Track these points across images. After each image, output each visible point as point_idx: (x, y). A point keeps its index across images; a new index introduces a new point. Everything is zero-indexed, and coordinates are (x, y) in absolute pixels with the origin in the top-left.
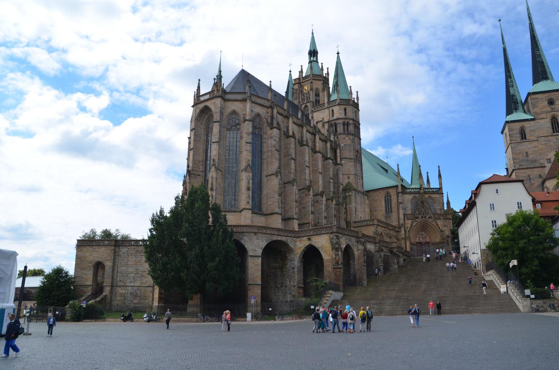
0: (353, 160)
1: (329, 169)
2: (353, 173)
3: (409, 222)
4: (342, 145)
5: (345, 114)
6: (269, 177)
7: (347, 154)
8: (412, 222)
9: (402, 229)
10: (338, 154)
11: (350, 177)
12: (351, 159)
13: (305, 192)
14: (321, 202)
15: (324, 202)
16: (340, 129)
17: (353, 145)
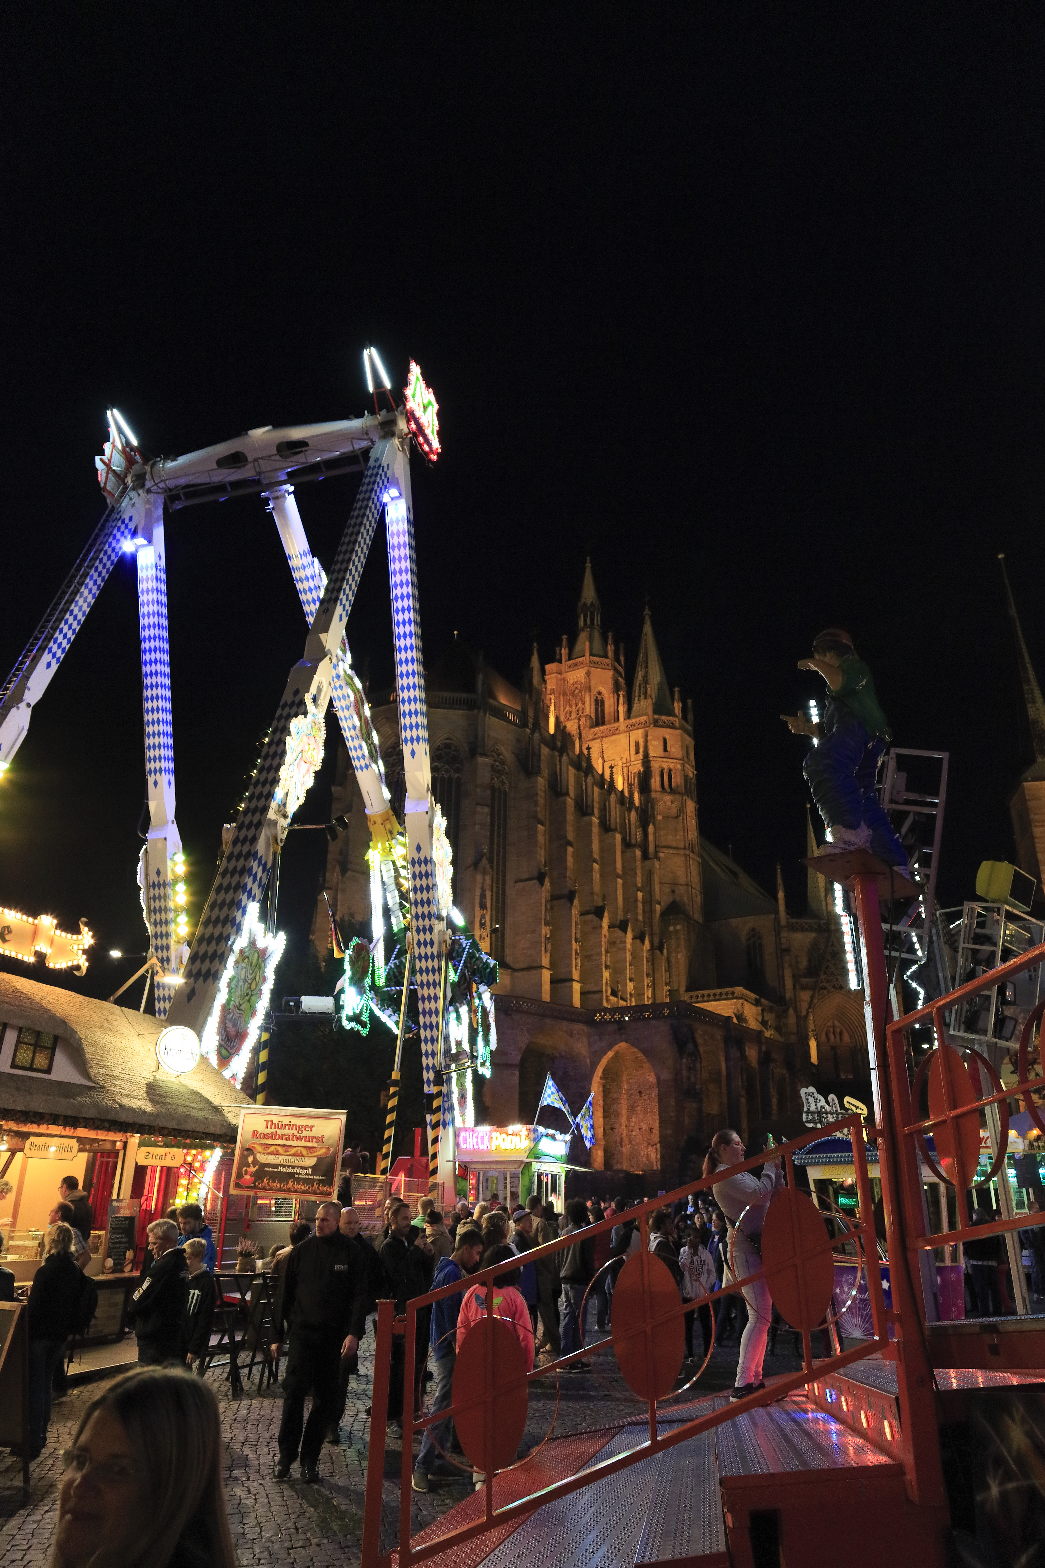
0: (682, 852)
1: (634, 870)
2: (682, 880)
3: (805, 996)
4: (660, 818)
5: (665, 750)
6: (521, 885)
7: (670, 837)
8: (812, 997)
9: (791, 1012)
10: (651, 837)
11: (677, 892)
12: (677, 848)
13: (592, 921)
14: (621, 946)
15: (629, 946)
16: (655, 783)
17: (683, 819)
